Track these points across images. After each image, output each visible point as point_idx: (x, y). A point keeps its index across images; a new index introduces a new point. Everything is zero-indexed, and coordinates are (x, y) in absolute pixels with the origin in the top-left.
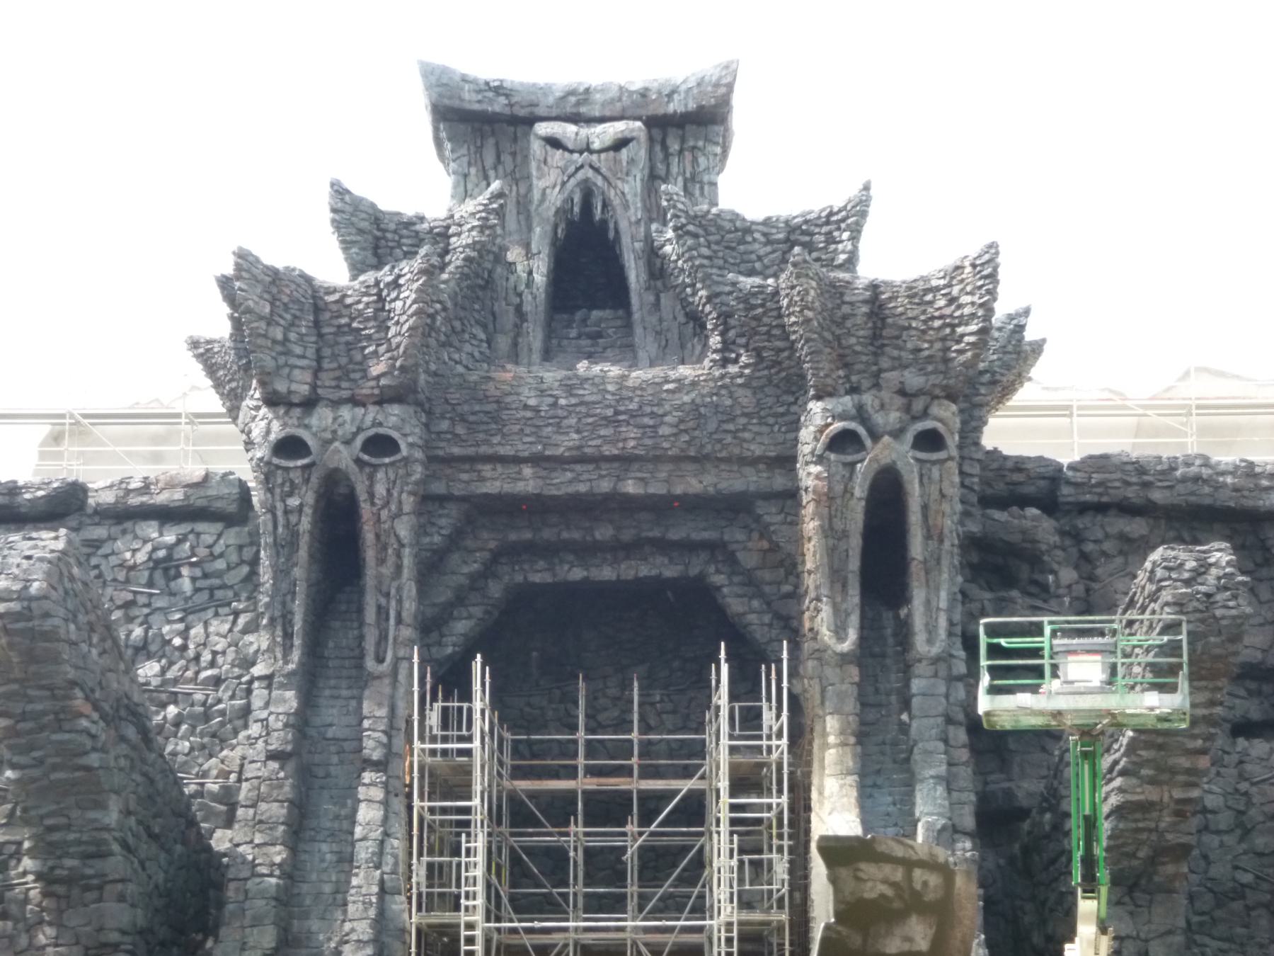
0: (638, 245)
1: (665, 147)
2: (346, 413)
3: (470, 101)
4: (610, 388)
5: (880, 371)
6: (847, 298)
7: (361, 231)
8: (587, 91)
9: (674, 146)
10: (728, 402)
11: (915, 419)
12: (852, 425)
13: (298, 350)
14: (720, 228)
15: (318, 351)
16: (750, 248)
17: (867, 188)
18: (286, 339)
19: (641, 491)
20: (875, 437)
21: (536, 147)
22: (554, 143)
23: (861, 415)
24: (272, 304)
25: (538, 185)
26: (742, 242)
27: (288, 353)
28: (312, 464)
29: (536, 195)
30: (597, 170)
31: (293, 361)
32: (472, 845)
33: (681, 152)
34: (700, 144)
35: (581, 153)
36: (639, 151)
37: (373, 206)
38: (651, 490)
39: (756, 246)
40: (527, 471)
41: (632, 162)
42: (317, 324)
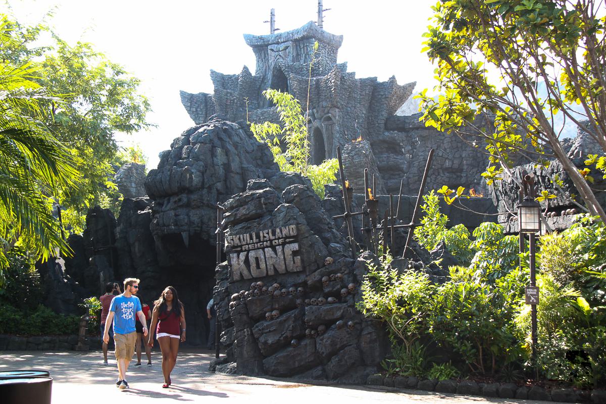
4: (271, 113)
5: (319, 102)
8: (281, 35)
11: (325, 114)
13: (201, 113)
14: (296, 68)
15: (206, 112)
16: (303, 72)
18: (196, 110)
21: (269, 51)
22: (272, 50)
24: (191, 103)
26: (301, 71)
27: (198, 114)
31: (200, 115)
33: (304, 47)
36: (290, 50)
37: (222, 74)
39: (305, 72)
41: (289, 52)
42: (206, 105)
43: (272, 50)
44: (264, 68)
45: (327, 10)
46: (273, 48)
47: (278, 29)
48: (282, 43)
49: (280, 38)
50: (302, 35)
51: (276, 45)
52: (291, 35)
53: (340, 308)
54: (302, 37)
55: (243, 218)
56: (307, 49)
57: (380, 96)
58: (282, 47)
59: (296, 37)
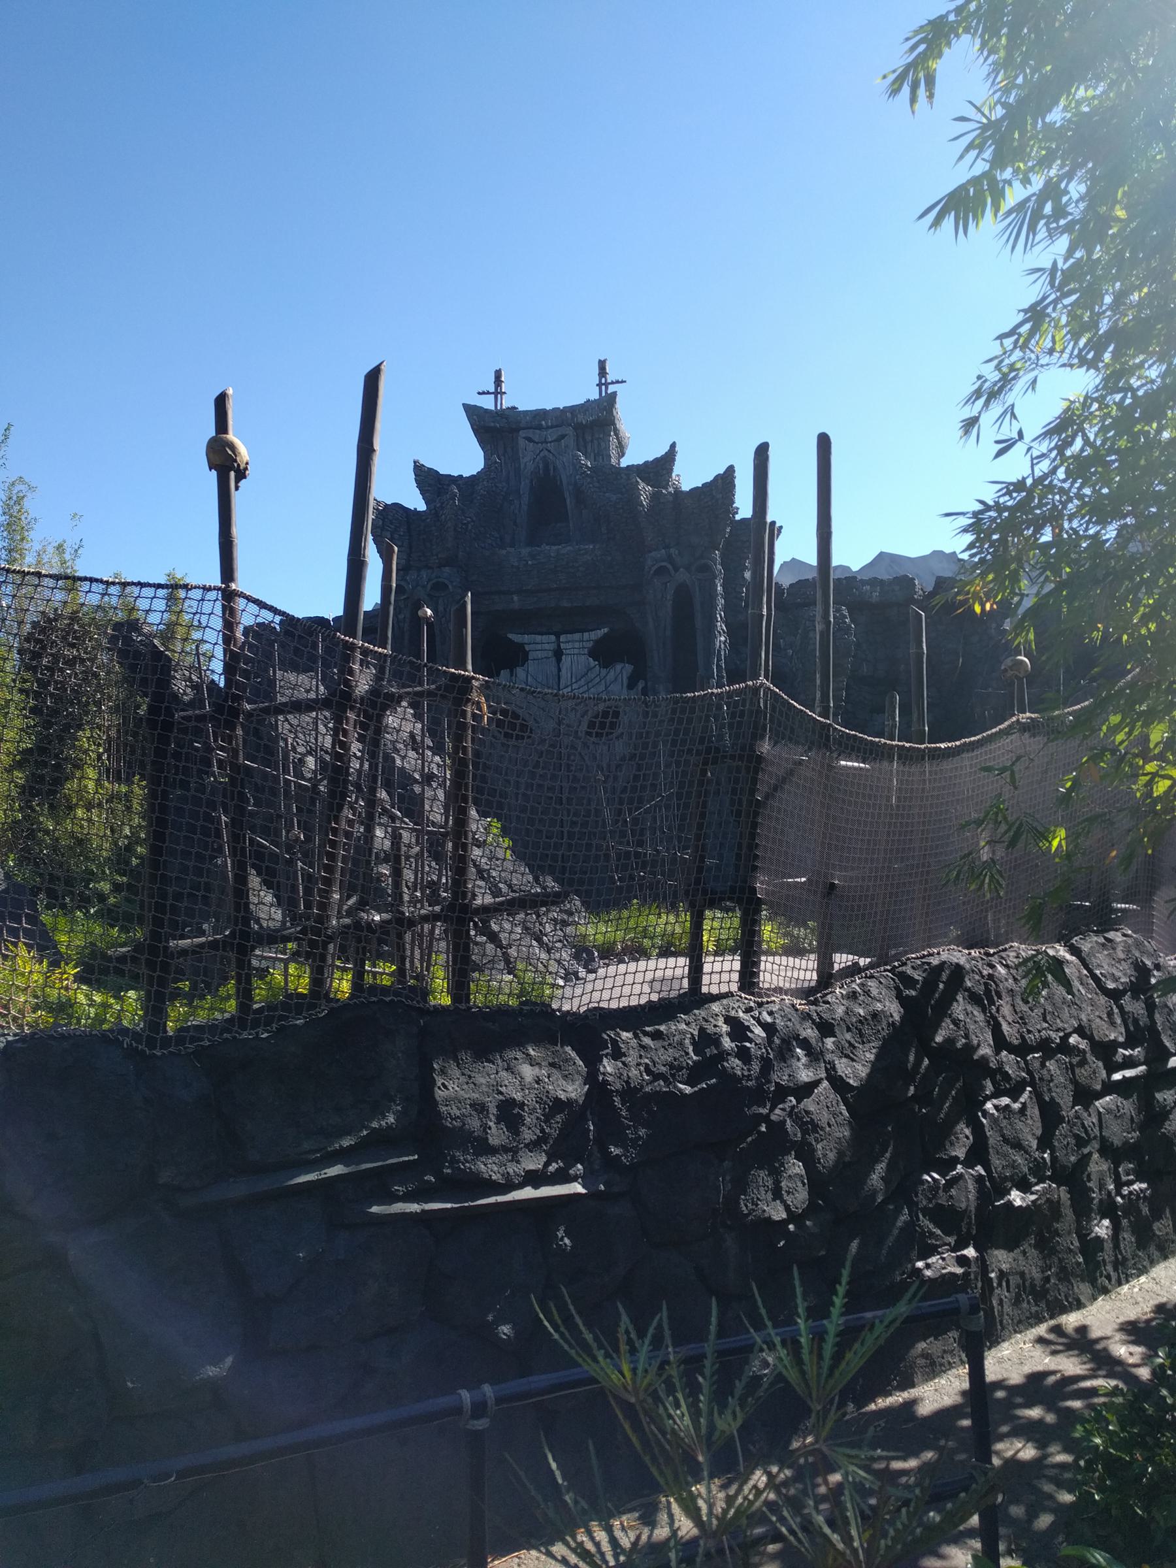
0: (571, 488)
2: (424, 574)
6: (662, 501)
7: (430, 485)
9: (589, 438)
10: (609, 558)
12: (663, 564)
17: (673, 446)
19: (570, 605)
20: (676, 570)
21: (522, 443)
22: (530, 440)
23: (670, 558)
24: (383, 520)
25: (523, 461)
28: (408, 598)
29: (522, 466)
30: (549, 451)
32: (625, 784)
33: (592, 441)
34: (601, 436)
35: (542, 443)
38: (575, 604)
40: (515, 598)
41: (566, 446)
43: (530, 440)
45: (618, 382)
48: (548, 428)
51: (538, 431)
56: (599, 444)
58: (552, 435)
59: (581, 418)
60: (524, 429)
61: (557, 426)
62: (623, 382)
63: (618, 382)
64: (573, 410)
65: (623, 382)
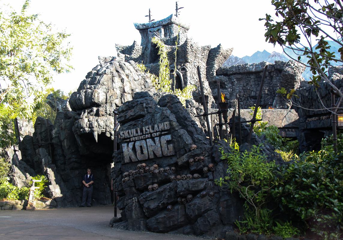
1: (166, 29)
3: (141, 27)
8: (155, 23)
9: (167, 29)
21: (149, 32)
22: (151, 31)
43: (151, 31)
44: (146, 42)
45: (181, 8)
46: (151, 30)
47: (153, 20)
49: (155, 24)
50: (167, 22)
51: (153, 29)
52: (161, 23)
53: (203, 182)
54: (167, 24)
55: (131, 118)
57: (213, 56)
58: (156, 29)
59: (164, 23)
60: (149, 28)
61: (158, 26)
62: (182, 8)
63: (181, 8)
64: (162, 21)
65: (182, 8)
